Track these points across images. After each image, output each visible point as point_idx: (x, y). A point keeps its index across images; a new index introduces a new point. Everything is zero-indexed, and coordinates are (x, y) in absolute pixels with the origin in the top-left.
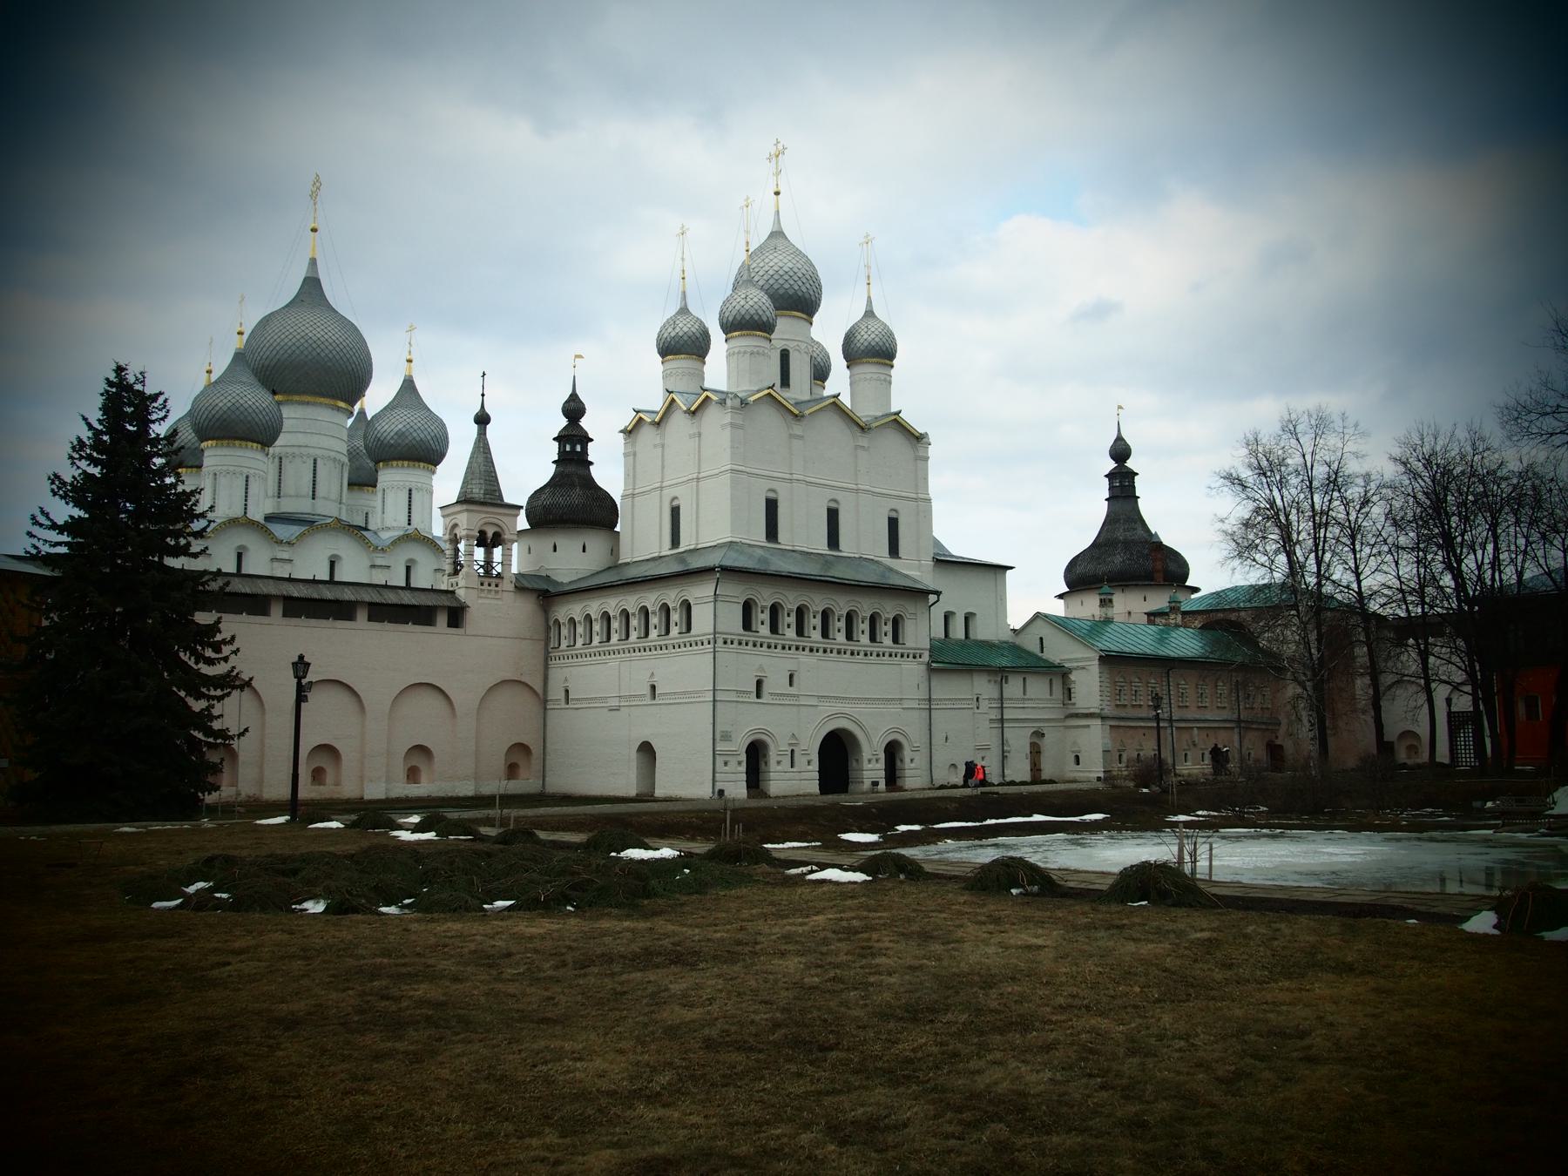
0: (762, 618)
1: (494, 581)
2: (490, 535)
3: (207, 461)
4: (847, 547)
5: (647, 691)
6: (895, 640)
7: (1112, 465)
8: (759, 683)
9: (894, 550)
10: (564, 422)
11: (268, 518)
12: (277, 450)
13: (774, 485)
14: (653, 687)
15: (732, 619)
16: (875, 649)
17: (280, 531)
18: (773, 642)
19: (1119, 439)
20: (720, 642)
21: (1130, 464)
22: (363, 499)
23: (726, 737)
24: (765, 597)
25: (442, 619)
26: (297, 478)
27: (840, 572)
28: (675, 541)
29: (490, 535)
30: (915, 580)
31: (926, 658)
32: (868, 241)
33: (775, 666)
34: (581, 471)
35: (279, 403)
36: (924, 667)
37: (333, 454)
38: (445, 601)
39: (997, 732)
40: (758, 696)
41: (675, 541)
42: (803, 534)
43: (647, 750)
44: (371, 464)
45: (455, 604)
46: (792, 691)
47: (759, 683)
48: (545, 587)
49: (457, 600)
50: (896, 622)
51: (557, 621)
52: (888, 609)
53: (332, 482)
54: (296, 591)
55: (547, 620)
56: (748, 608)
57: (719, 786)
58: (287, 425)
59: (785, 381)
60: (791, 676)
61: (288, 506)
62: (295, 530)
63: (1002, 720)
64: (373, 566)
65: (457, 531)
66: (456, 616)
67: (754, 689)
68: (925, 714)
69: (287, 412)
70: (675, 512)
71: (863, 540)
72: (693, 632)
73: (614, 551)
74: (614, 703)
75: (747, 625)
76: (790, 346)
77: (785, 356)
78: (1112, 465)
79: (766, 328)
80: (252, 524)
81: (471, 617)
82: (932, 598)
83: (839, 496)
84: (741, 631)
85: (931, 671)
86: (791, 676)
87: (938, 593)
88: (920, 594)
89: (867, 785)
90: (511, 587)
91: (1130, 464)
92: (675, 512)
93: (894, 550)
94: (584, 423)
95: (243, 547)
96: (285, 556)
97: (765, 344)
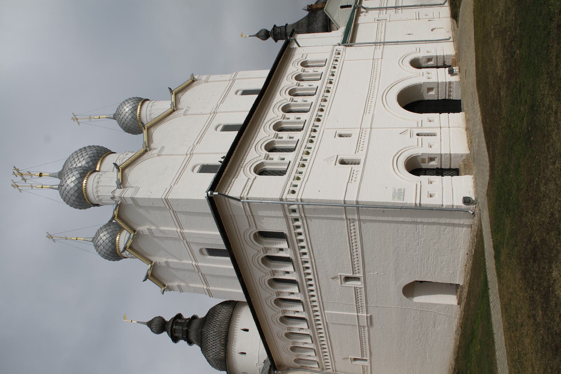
7: (271, 39)
14: (347, 279)
15: (269, 189)
19: (258, 35)
21: (270, 29)
23: (401, 193)
34: (195, 325)
39: (405, 11)
40: (357, 163)
43: (411, 289)
46: (355, 134)
51: (296, 361)
55: (296, 369)
57: (459, 203)
63: (396, 8)
67: (349, 167)
68: (387, 47)
72: (286, 232)
74: (364, 322)
78: (271, 39)
83: (215, 123)
89: (455, 79)
91: (270, 29)
94: (168, 318)
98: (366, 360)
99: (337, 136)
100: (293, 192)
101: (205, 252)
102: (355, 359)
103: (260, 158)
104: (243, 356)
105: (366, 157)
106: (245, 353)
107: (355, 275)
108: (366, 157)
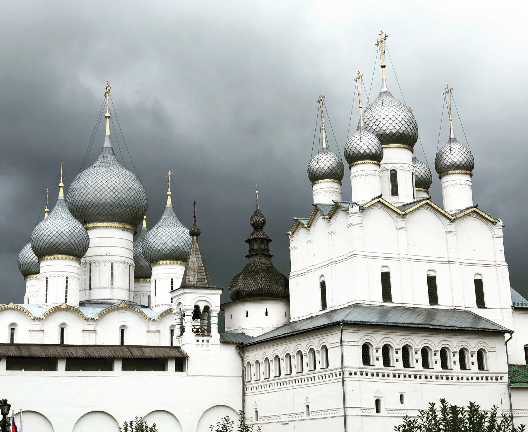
0: (376, 356)
1: (205, 339)
2: (202, 309)
3: (41, 271)
4: (445, 300)
5: (305, 409)
6: (481, 367)
8: (378, 402)
9: (481, 302)
10: (252, 229)
11: (82, 304)
12: (88, 260)
13: (386, 263)
15: (354, 357)
16: (465, 374)
17: (90, 312)
18: (386, 372)
20: (347, 374)
22: (143, 286)
24: (378, 340)
25: (171, 366)
26: (101, 275)
27: (441, 321)
28: (324, 305)
29: (202, 309)
30: (494, 324)
31: (506, 379)
32: (449, 91)
33: (389, 390)
35: (87, 229)
36: (504, 388)
37: (123, 259)
38: (174, 353)
40: (378, 411)
41: (324, 305)
42: (410, 293)
44: (147, 263)
45: (179, 355)
46: (401, 406)
47: (378, 402)
48: (240, 341)
49: (181, 353)
50: (480, 354)
51: (249, 363)
52: (473, 345)
53: (124, 276)
54: (75, 353)
56: (366, 348)
58: (92, 243)
59: (395, 191)
60: (402, 396)
61: (96, 295)
62: (98, 310)
64: (148, 331)
65: (181, 306)
66: (181, 363)
67: (374, 406)
69: (92, 234)
70: (323, 285)
71: (456, 295)
72: (329, 368)
73: (288, 314)
74: (285, 419)
75: (366, 361)
76: (396, 167)
77: (394, 175)
79: (376, 158)
80: (70, 309)
81: (190, 365)
82: (507, 336)
84: (362, 365)
85: (511, 389)
86: (402, 396)
87: (511, 332)
88: (498, 333)
90: (218, 342)
92: (323, 285)
93: (481, 302)
95: (63, 324)
96: (91, 328)
97: (376, 168)
98: (257, 420)
99: (400, 394)
100: (351, 374)
101: (322, 279)
102: (257, 411)
103: (376, 344)
104: (245, 315)
105: (383, 417)
106: (247, 316)
107: (310, 413)
108: (383, 417)
